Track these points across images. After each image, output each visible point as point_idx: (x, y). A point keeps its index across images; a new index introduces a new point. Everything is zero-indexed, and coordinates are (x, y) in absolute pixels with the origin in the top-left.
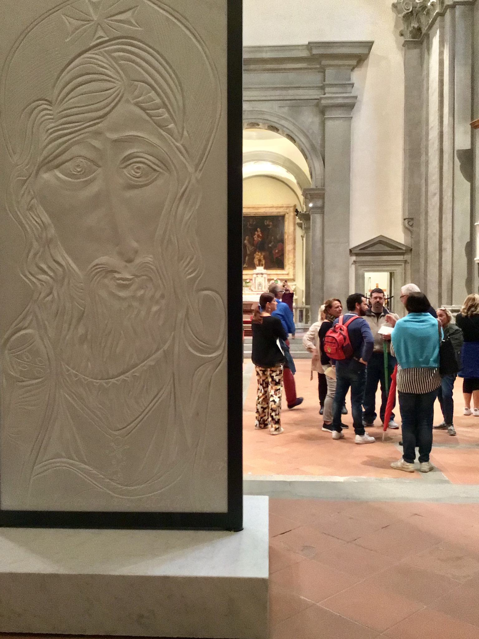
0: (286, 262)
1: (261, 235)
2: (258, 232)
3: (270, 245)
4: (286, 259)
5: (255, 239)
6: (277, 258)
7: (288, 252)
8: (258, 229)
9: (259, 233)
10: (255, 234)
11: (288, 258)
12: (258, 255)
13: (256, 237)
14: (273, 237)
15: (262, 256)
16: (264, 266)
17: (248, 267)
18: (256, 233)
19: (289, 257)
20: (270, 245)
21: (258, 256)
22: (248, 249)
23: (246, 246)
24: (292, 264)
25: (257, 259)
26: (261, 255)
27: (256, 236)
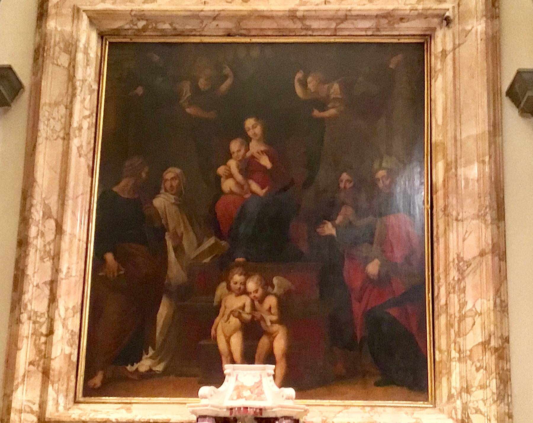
0: (442, 342)
1: (265, 162)
2: (247, 140)
3: (329, 229)
4: (442, 321)
5: (228, 185)
6: (368, 314)
7: (454, 274)
8: (250, 123)
9: (255, 147)
10: (229, 155)
11: (454, 309)
12: (245, 292)
13: (230, 176)
14: (345, 176)
15: (271, 301)
16: (282, 364)
17: (166, 372)
18: (235, 146)
19: (463, 305)
20: (329, 229)
21: (245, 300)
22: (179, 249)
23: (164, 229)
24: (490, 359)
25: (234, 321)
26: (266, 295)
27: (233, 164)
